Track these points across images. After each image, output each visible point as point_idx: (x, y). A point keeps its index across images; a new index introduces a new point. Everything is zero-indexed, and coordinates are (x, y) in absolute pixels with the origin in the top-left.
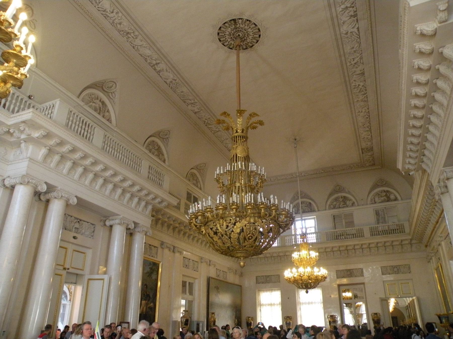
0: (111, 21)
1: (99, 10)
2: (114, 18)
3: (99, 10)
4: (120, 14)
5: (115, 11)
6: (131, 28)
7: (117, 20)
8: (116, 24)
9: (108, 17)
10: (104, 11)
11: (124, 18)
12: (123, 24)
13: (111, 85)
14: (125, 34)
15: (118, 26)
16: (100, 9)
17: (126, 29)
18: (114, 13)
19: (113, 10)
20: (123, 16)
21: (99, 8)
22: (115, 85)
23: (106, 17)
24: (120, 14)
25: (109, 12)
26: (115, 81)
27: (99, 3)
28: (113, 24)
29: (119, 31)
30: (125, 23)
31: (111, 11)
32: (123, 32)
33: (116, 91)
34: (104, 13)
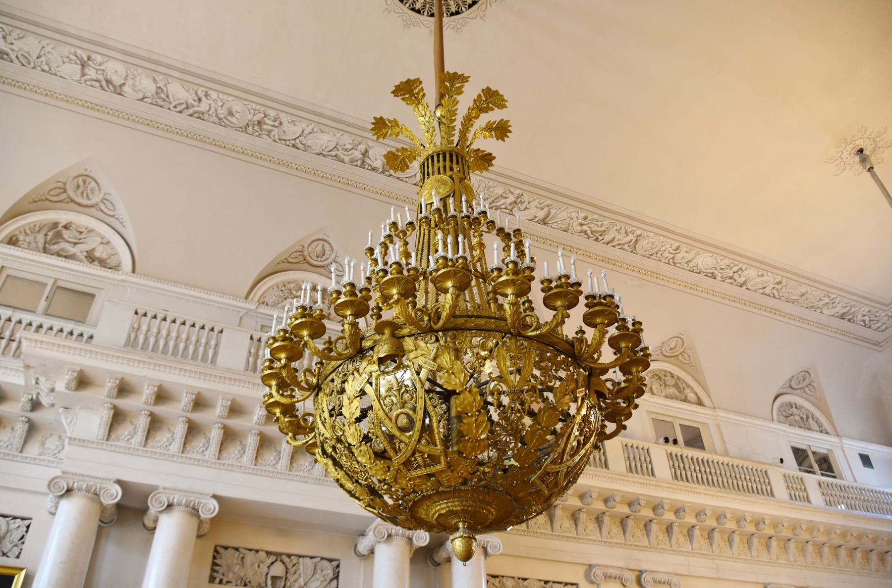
0: (214, 119)
1: (180, 112)
2: (213, 110)
3: (180, 112)
4: (214, 95)
5: (201, 94)
6: (255, 110)
7: (220, 111)
8: (226, 118)
9: (203, 113)
10: (187, 108)
11: (225, 97)
12: (234, 110)
13: (319, 248)
14: (256, 128)
15: (233, 120)
16: (179, 108)
17: (250, 117)
18: (204, 99)
19: (196, 94)
20: (221, 95)
21: (175, 107)
22: (326, 245)
23: (200, 116)
24: (214, 95)
25: (196, 104)
26: (321, 237)
27: (168, 97)
28: (220, 122)
29: (244, 129)
30: (237, 107)
31: (196, 98)
32: (251, 128)
33: (336, 257)
34: (191, 111)
